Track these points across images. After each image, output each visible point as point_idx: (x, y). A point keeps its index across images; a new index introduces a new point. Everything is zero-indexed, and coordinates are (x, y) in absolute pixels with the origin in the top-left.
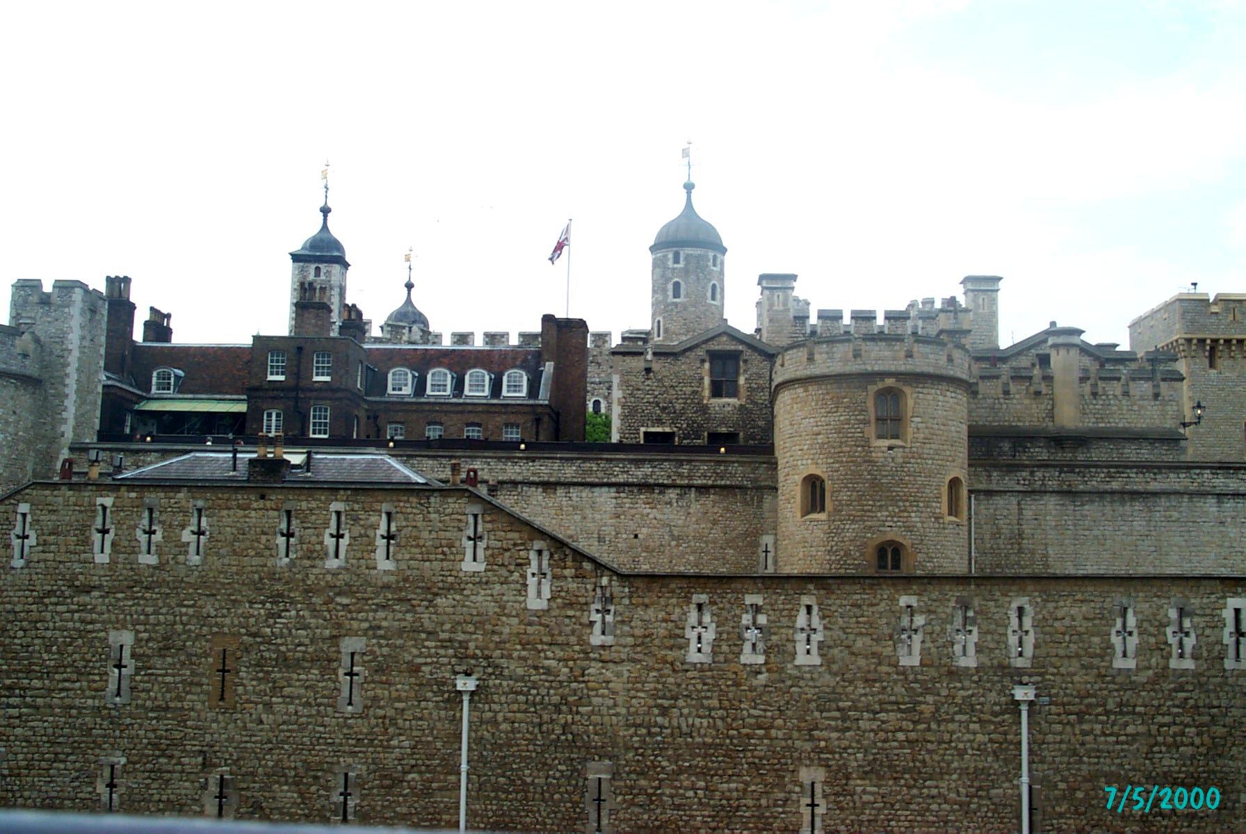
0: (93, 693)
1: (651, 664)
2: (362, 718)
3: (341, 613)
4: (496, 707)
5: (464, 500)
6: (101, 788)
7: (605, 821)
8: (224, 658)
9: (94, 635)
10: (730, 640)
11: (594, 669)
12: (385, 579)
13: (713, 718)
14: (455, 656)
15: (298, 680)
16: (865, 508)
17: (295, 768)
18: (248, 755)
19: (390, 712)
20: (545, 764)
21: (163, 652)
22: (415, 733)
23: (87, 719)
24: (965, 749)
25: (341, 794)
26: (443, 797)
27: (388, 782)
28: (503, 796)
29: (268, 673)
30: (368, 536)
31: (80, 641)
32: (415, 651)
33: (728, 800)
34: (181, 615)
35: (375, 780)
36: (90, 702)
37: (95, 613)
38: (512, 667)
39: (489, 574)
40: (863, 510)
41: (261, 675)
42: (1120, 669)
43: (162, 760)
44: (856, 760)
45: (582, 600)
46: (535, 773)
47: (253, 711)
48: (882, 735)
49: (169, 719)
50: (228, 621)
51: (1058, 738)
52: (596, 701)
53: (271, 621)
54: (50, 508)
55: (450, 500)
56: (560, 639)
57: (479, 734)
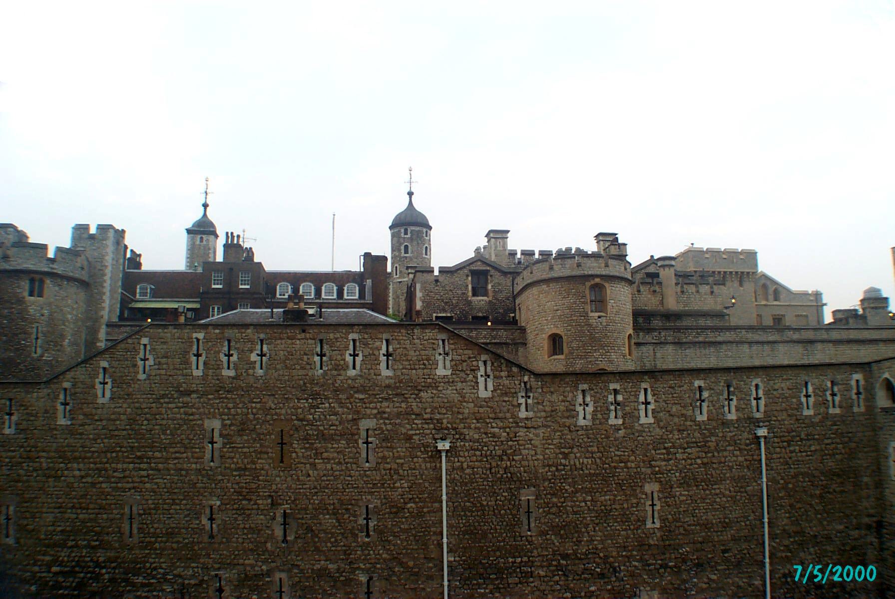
0: (196, 460)
1: (556, 428)
2: (375, 470)
3: (358, 405)
4: (462, 459)
6: (205, 521)
7: (532, 525)
8: (282, 436)
9: (194, 422)
10: (602, 412)
11: (522, 433)
12: (387, 382)
13: (594, 458)
14: (435, 429)
15: (332, 448)
17: (334, 504)
18: (301, 497)
19: (395, 466)
20: (495, 492)
21: (241, 432)
22: (410, 478)
24: (733, 466)
25: (364, 519)
26: (430, 517)
27: (394, 510)
28: (469, 514)
29: (312, 444)
31: (185, 426)
32: (408, 427)
33: (605, 506)
34: (252, 408)
36: (194, 466)
38: (471, 434)
39: (454, 376)
41: (307, 446)
42: (806, 416)
44: (675, 477)
45: (513, 391)
46: (489, 498)
47: (303, 469)
48: (689, 461)
49: (247, 476)
50: (283, 411)
51: (779, 456)
52: (524, 452)
53: (313, 411)
54: (162, 340)
56: (501, 415)
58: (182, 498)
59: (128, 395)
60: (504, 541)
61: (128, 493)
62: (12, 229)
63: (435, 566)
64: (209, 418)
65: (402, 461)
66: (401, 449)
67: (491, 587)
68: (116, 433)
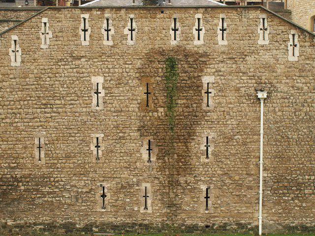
4: (276, 105)
5: (259, 12)
6: (93, 148)
9: (84, 79)
12: (223, 49)
14: (256, 83)
17: (183, 136)
22: (238, 118)
23: (84, 117)
25: (205, 146)
27: (227, 140)
32: (238, 82)
34: (125, 68)
36: (84, 110)
39: (271, 45)
43: (121, 135)
49: (122, 116)
50: (148, 70)
54: (58, 20)
56: (303, 74)
58: (76, 132)
59: (34, 60)
60: (302, 163)
61: (37, 130)
63: (254, 180)
64: (95, 76)
66: (232, 97)
67: (292, 195)
68: (27, 87)
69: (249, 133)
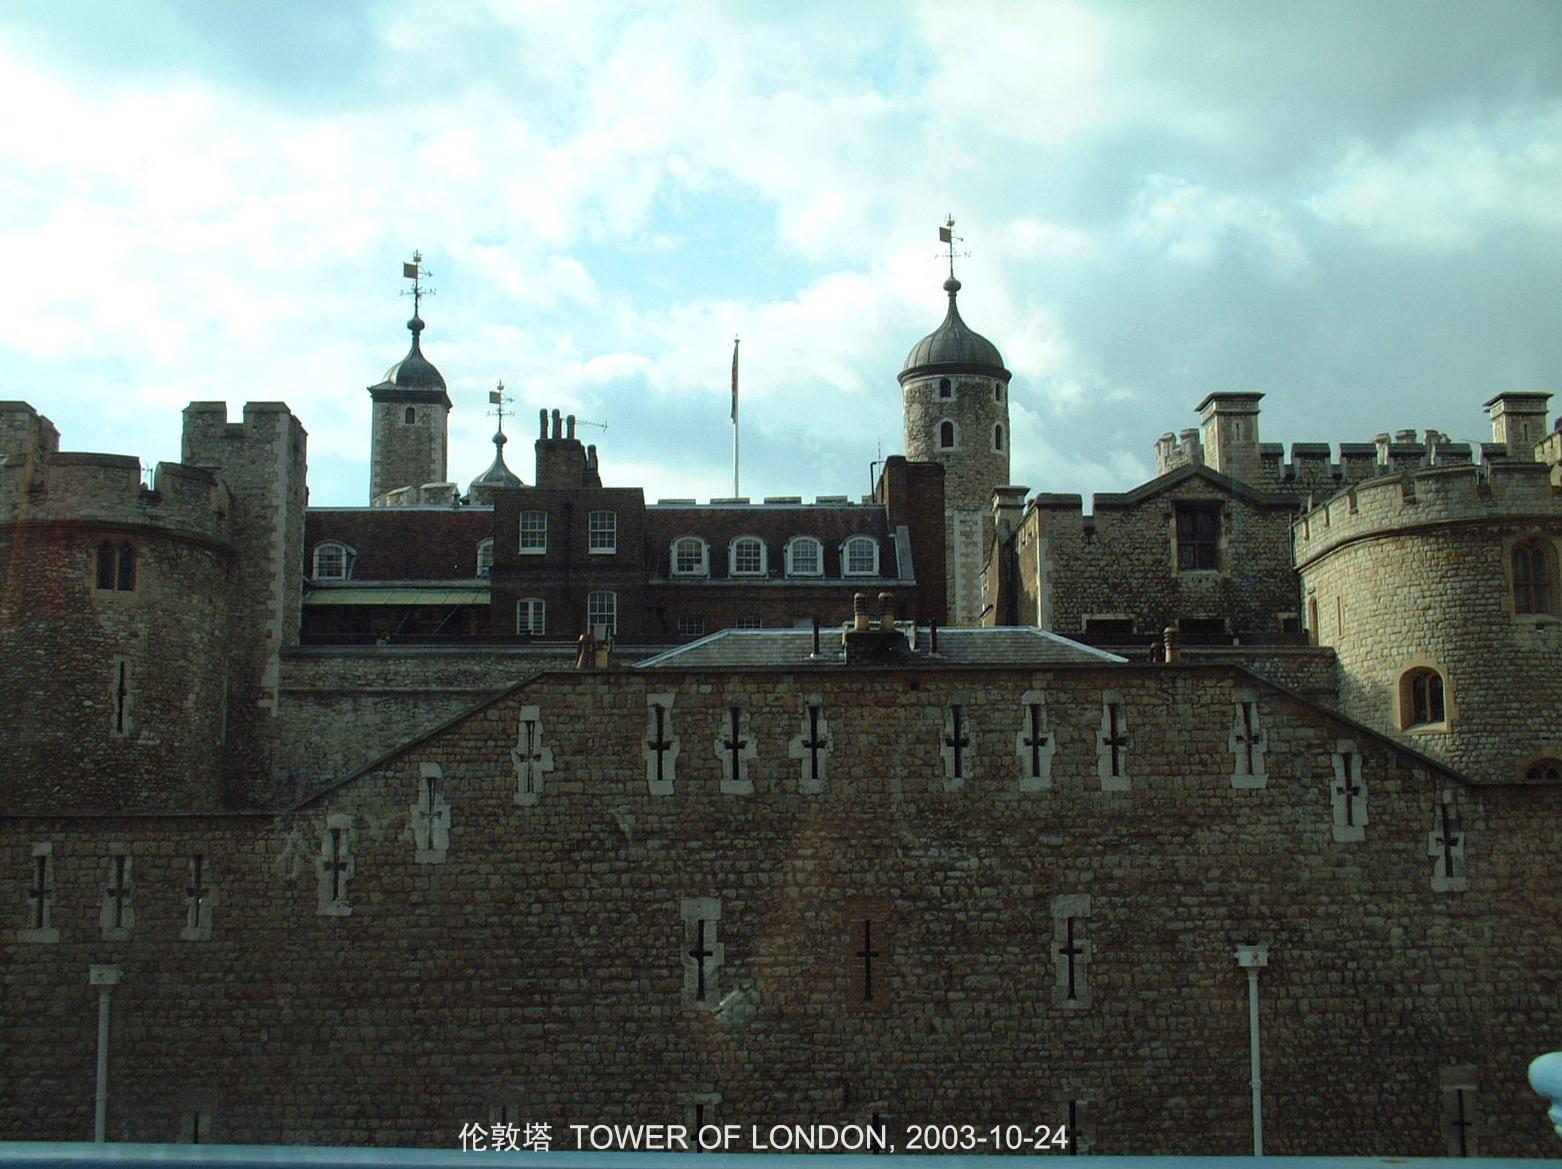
4: (1297, 991)
5: (1229, 682)
11: (1439, 927)
12: (1116, 805)
14: (1230, 916)
15: (988, 964)
16: (1508, 713)
17: (992, 1098)
19: (1135, 1007)
22: (1174, 1036)
23: (653, 1037)
27: (1138, 1112)
29: (940, 954)
30: (1084, 741)
34: (794, 870)
35: (1117, 1108)
36: (656, 1010)
37: (657, 872)
38: (1317, 931)
39: (1274, 792)
40: (1505, 716)
41: (928, 958)
43: (779, 1095)
45: (1415, 826)
47: (919, 1014)
50: (870, 878)
52: (1446, 974)
54: (572, 712)
55: (1207, 683)
56: (1385, 885)
57: (1275, 1032)
58: (628, 1086)
59: (492, 842)
61: (498, 1079)
62: (26, 417)
65: (1151, 995)
69: (1215, 1087)
